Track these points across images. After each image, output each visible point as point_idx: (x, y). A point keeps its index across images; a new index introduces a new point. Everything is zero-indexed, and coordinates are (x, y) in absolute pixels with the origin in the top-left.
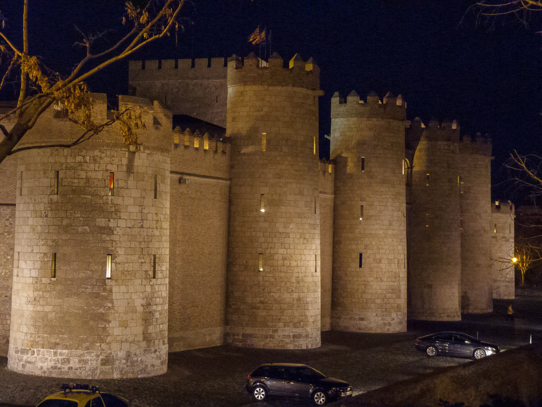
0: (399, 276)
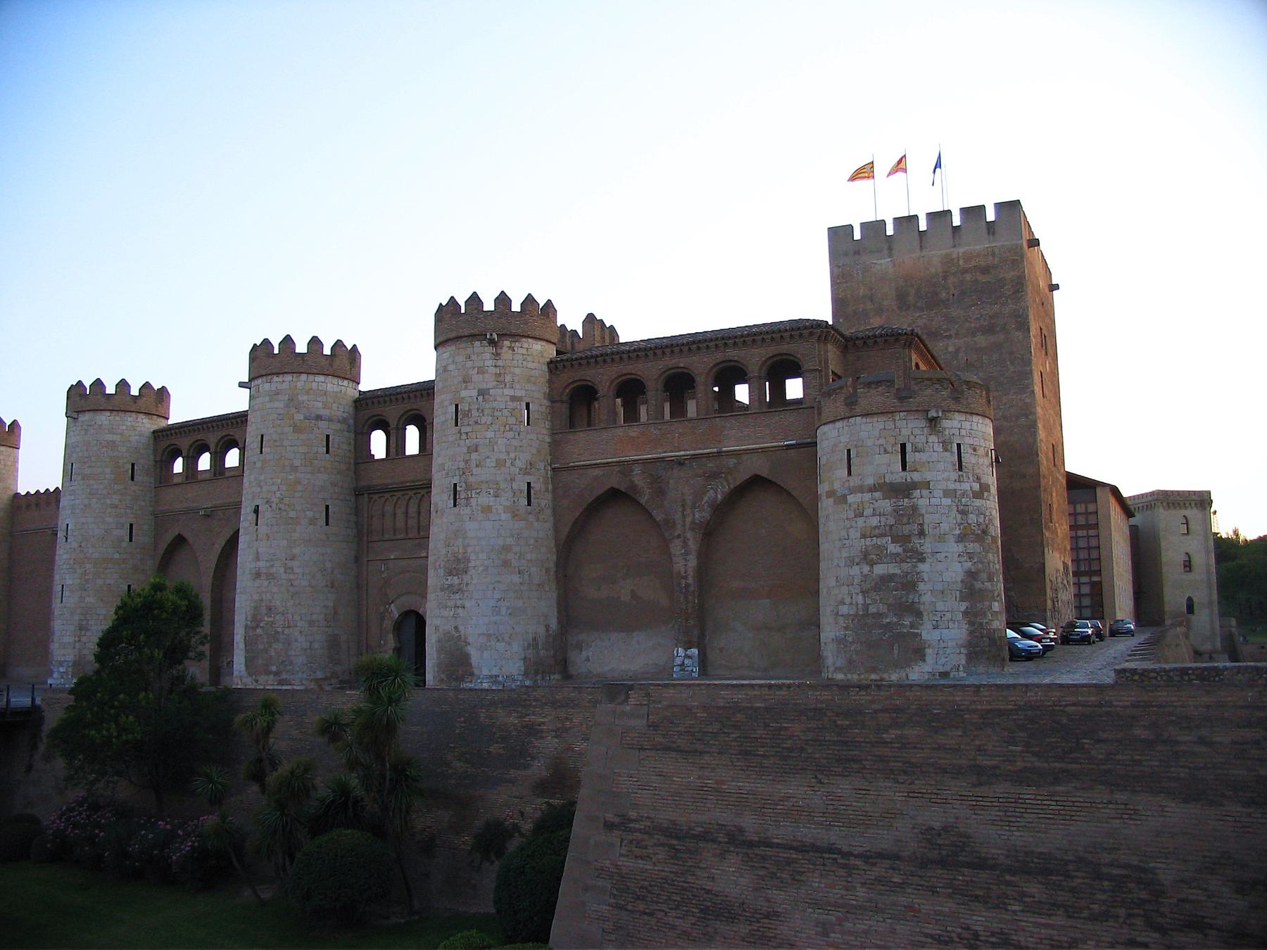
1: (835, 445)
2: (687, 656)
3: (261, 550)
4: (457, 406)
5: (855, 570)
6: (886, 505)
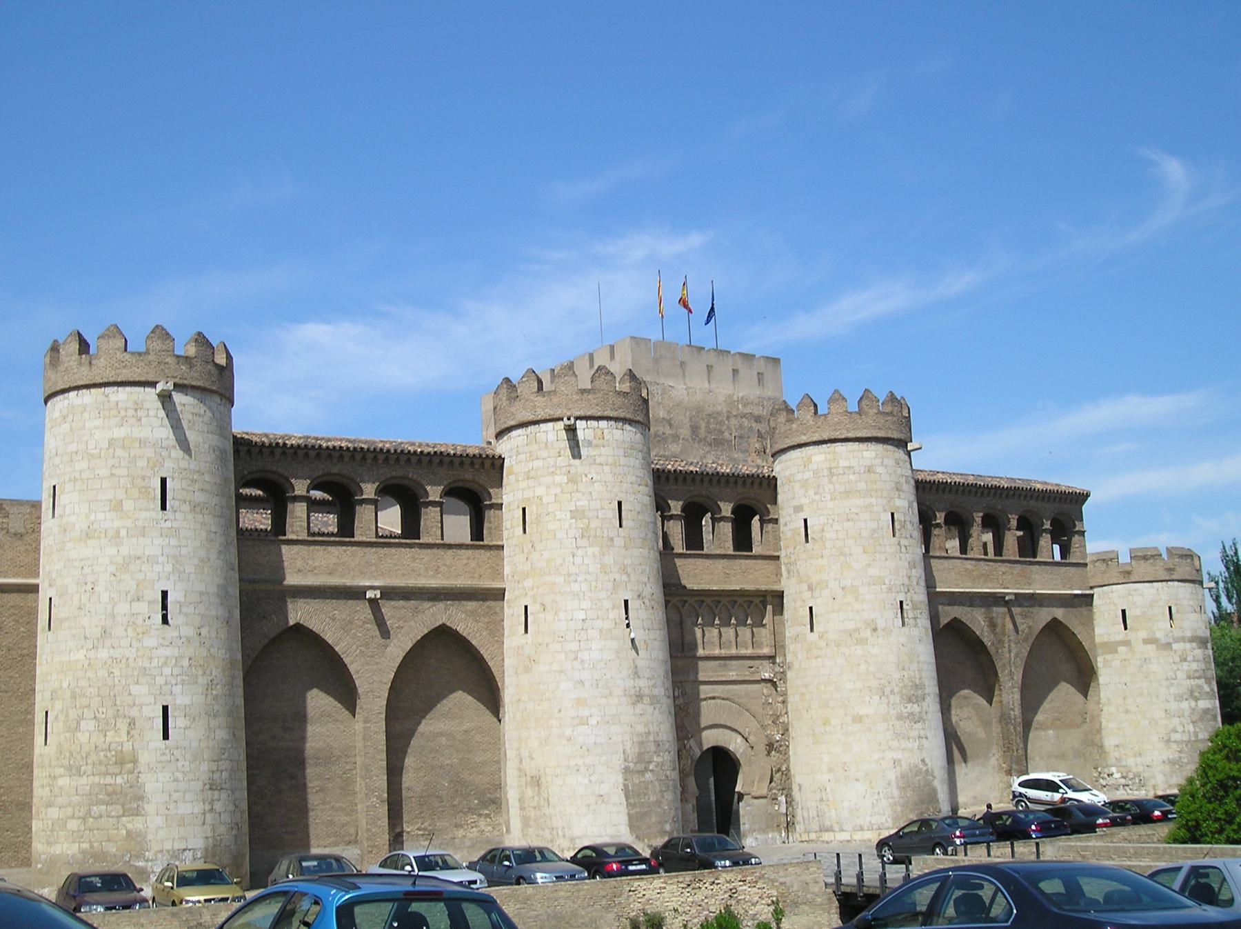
0: (135, 761)
4: (892, 514)
5: (1185, 705)
6: (1199, 653)
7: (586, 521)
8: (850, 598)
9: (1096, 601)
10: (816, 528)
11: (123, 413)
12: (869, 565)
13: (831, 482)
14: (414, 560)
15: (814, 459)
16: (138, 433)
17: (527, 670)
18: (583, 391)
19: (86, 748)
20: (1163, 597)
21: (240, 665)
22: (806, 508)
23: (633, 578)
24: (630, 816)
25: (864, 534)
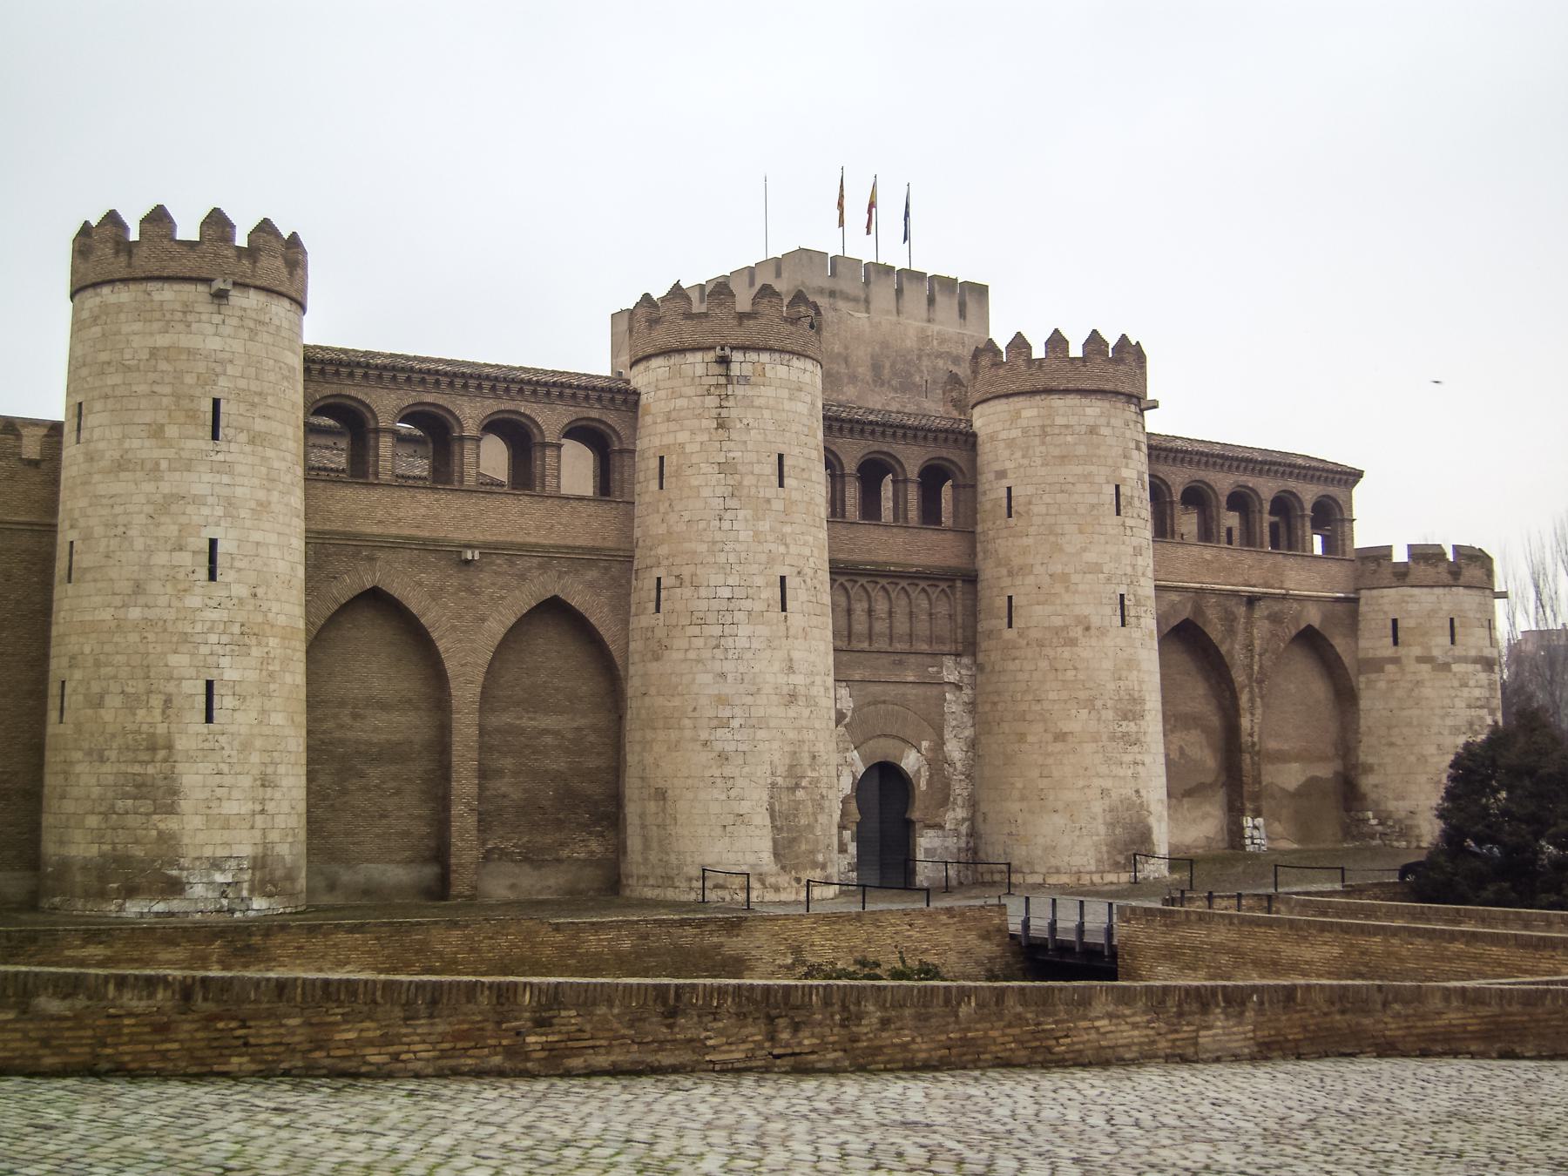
0: (170, 747)
1: (1434, 611)
2: (1255, 827)
3: (796, 655)
4: (1117, 487)
7: (737, 477)
8: (1058, 588)
9: (1363, 608)
10: (1021, 500)
11: (168, 316)
12: (1084, 550)
13: (1043, 443)
14: (522, 514)
15: (1026, 413)
16: (185, 341)
17: (657, 659)
18: (742, 316)
19: (110, 729)
20: (1445, 607)
21: (302, 636)
22: (1010, 475)
23: (793, 549)
24: (775, 841)
25: (1082, 510)
